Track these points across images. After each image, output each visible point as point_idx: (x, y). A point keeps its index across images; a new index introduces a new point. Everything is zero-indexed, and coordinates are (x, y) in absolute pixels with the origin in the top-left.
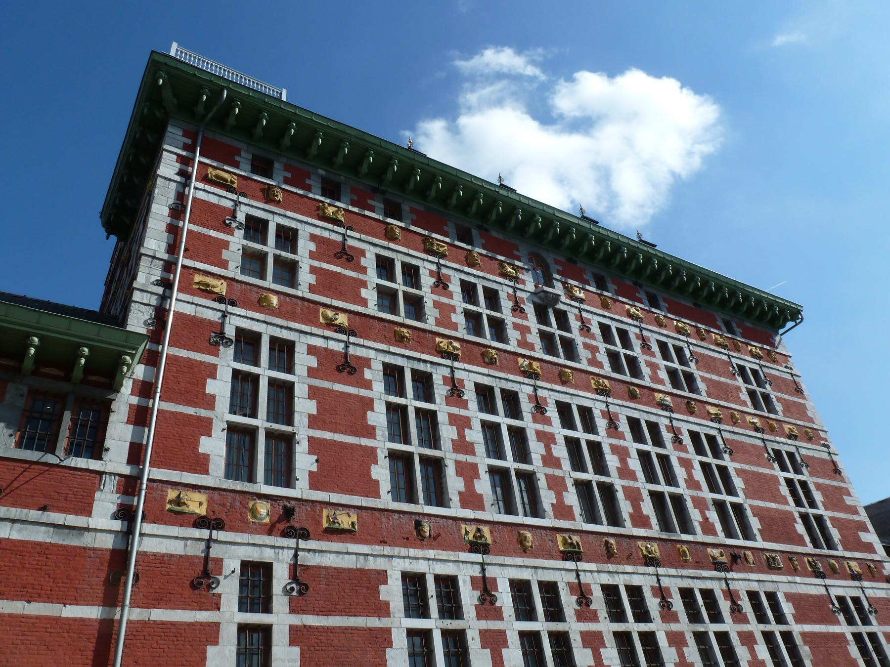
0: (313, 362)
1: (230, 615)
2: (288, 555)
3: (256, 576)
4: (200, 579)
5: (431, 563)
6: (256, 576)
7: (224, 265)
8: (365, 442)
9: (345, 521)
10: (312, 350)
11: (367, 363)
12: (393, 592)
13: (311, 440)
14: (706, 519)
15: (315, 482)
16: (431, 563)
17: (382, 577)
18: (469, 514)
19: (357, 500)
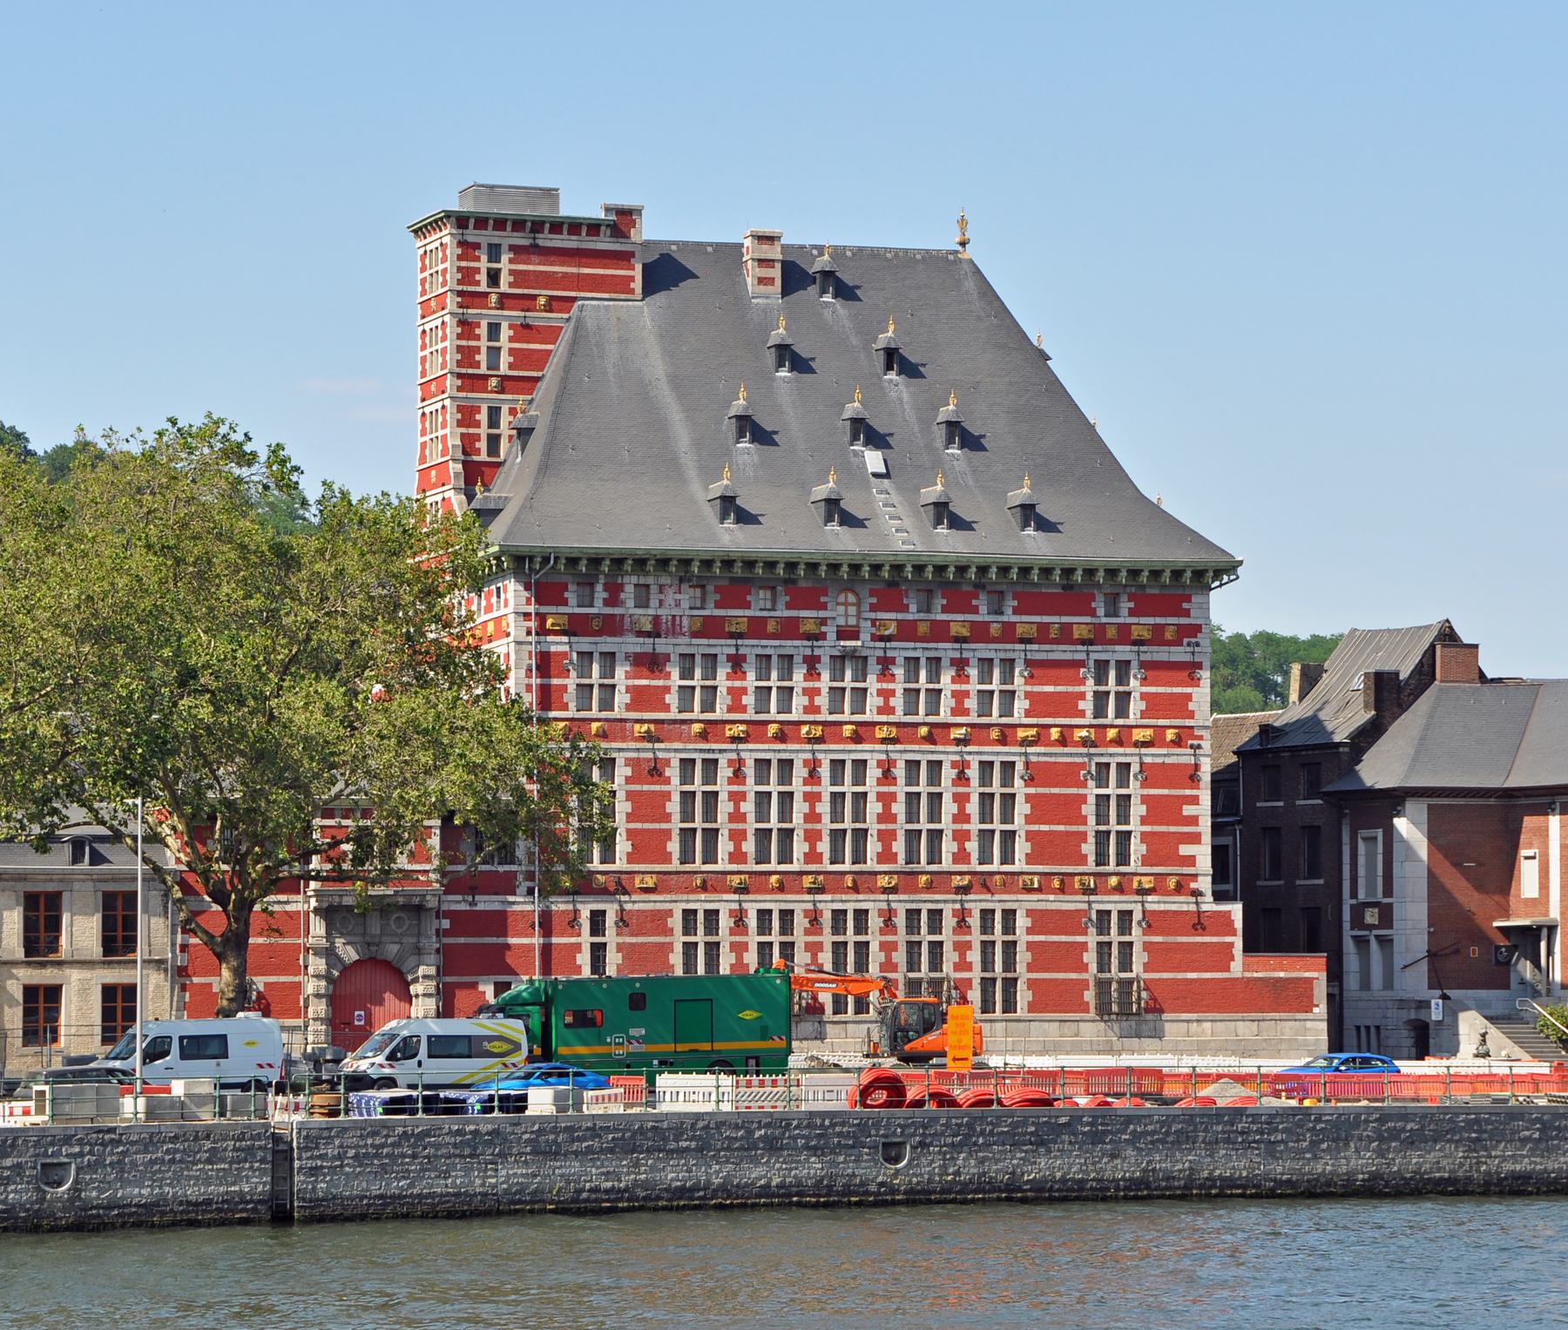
0: (628, 771)
1: (586, 939)
2: (616, 906)
3: (597, 919)
4: (573, 922)
5: (701, 903)
6: (597, 919)
7: (565, 707)
8: (664, 826)
9: (650, 882)
10: (628, 762)
11: (667, 762)
12: (676, 922)
13: (628, 831)
14: (962, 849)
15: (631, 858)
16: (701, 903)
17: (670, 913)
18: (734, 867)
19: (658, 868)
